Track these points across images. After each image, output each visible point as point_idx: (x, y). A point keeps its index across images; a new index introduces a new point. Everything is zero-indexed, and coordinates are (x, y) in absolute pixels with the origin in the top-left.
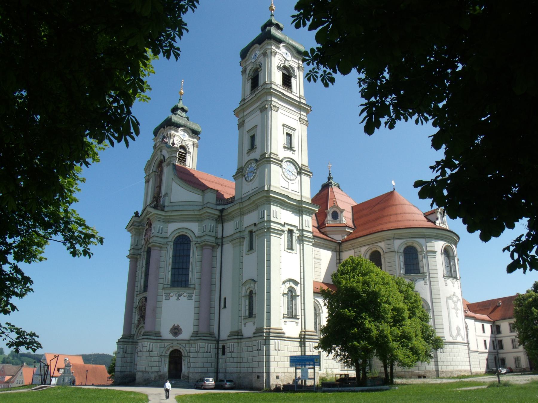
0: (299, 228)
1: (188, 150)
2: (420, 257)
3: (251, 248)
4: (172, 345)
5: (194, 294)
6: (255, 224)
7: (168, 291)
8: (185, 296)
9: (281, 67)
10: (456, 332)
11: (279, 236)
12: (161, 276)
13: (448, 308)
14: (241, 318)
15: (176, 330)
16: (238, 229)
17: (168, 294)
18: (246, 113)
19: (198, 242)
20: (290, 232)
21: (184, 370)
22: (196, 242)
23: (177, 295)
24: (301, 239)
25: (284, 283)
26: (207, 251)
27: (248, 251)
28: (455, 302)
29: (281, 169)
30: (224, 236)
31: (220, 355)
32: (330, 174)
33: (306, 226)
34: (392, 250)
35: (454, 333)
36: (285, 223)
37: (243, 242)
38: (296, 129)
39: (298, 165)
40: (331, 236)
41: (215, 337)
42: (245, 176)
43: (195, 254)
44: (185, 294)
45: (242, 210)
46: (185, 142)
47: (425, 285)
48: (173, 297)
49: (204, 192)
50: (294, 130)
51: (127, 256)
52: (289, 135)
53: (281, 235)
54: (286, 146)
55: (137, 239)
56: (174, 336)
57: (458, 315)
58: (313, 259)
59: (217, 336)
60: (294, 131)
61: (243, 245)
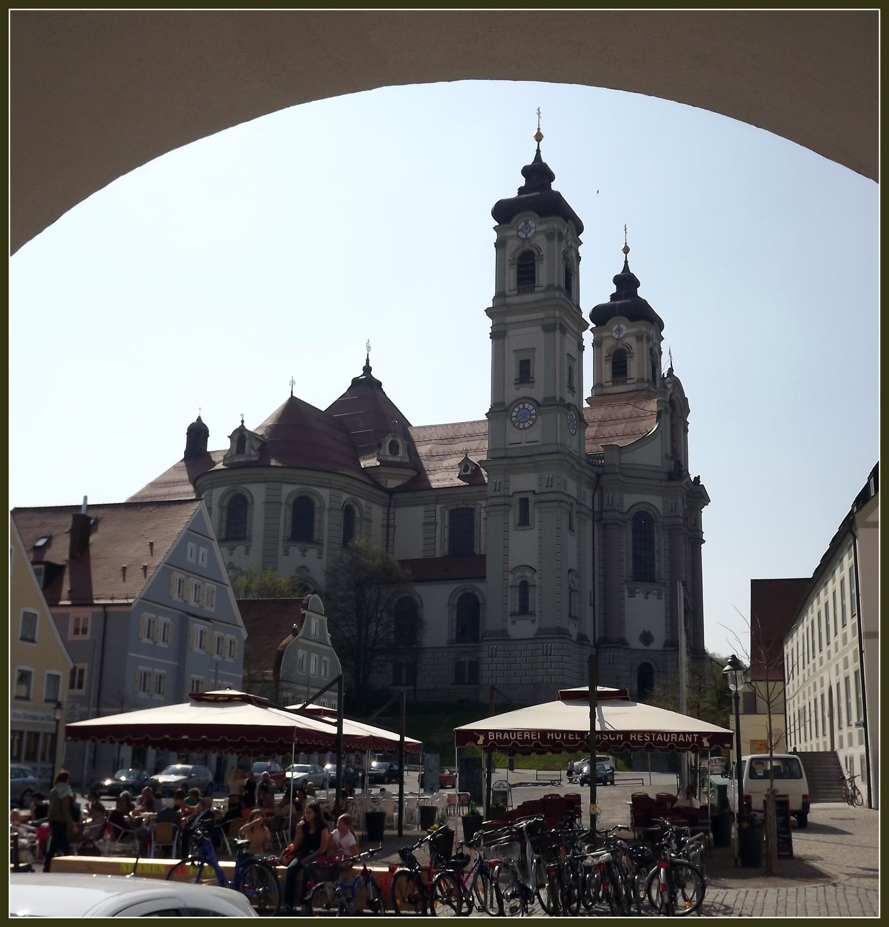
43: (660, 539)
44: (654, 592)
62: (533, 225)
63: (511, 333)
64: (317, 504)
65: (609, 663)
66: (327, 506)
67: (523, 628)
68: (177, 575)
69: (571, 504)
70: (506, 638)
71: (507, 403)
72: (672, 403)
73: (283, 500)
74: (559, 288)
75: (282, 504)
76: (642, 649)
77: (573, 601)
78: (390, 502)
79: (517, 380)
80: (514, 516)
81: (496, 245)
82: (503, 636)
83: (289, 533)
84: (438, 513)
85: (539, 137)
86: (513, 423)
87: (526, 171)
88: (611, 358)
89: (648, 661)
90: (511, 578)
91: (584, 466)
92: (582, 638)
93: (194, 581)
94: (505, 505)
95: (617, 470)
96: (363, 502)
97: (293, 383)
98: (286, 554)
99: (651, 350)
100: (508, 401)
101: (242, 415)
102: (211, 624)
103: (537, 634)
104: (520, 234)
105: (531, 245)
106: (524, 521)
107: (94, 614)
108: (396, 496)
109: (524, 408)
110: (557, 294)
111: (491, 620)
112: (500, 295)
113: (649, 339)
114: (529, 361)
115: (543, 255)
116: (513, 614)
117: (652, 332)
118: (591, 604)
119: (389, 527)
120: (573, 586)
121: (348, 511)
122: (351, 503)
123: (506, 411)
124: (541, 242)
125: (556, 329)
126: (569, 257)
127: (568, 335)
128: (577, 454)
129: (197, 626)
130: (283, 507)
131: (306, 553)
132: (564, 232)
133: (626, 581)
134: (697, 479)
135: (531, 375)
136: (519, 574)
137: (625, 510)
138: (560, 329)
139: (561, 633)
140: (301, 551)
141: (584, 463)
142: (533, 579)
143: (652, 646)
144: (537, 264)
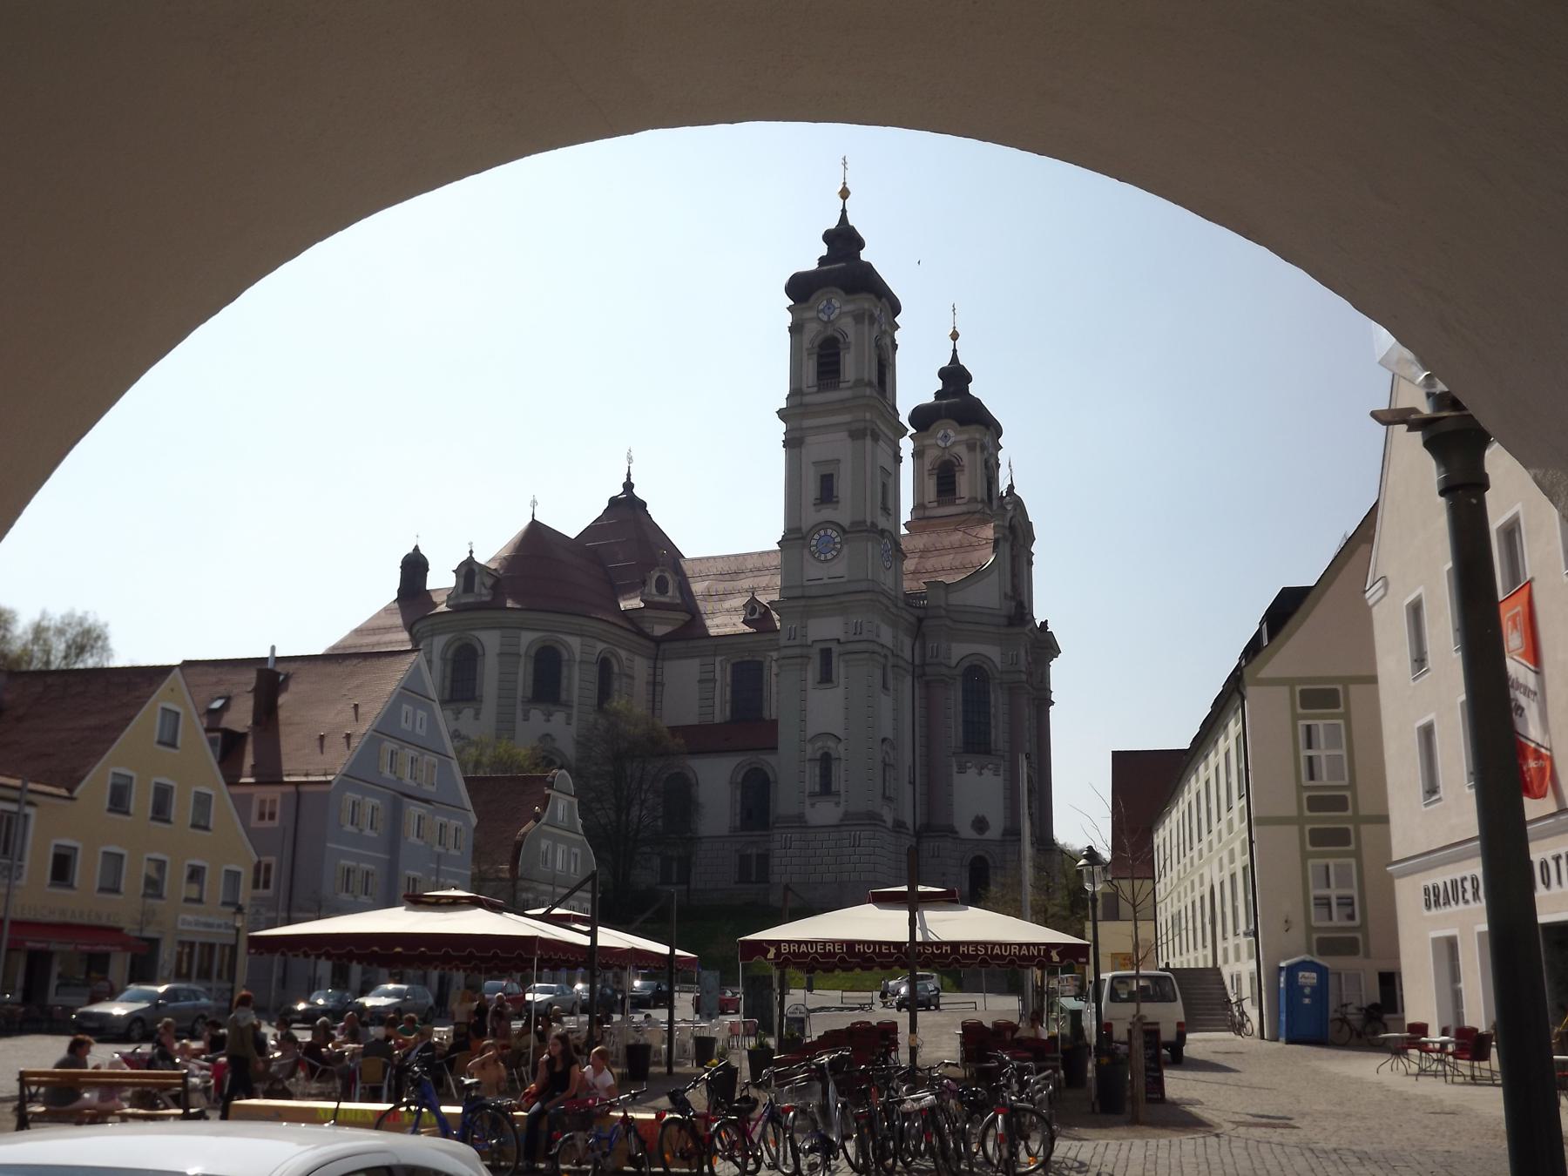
43: (998, 700)
44: (990, 766)
56: (979, 834)
62: (837, 305)
63: (809, 440)
64: (565, 656)
65: (933, 857)
66: (578, 658)
67: (824, 813)
68: (389, 745)
69: (885, 656)
70: (803, 825)
71: (805, 529)
72: (1012, 528)
73: (522, 651)
74: (870, 384)
75: (520, 656)
76: (975, 838)
77: (887, 778)
78: (657, 655)
79: (817, 499)
80: (813, 671)
81: (791, 329)
82: (800, 822)
83: (529, 694)
84: (718, 668)
85: (845, 194)
86: (813, 555)
87: (829, 237)
88: (935, 472)
89: (981, 853)
90: (809, 748)
91: (902, 609)
92: (899, 825)
93: (410, 752)
94: (802, 657)
95: (943, 613)
96: (623, 654)
97: (534, 503)
98: (526, 719)
99: (986, 462)
100: (805, 527)
101: (471, 544)
102: (431, 807)
103: (842, 820)
104: (821, 315)
105: (834, 330)
106: (826, 678)
107: (284, 795)
108: (664, 646)
109: (826, 535)
110: (868, 391)
111: (785, 801)
112: (795, 393)
113: (983, 448)
114: (832, 475)
115: (849, 343)
116: (812, 795)
117: (987, 440)
118: (910, 783)
119: (655, 684)
120: (887, 759)
121: (604, 665)
122: (609, 655)
123: (803, 538)
124: (848, 325)
125: (866, 435)
126: (883, 344)
127: (881, 443)
128: (893, 593)
129: (414, 810)
130: (522, 660)
131: (551, 718)
132: (877, 313)
133: (954, 753)
134: (1044, 624)
135: (835, 494)
136: (819, 744)
137: (953, 662)
138: (872, 436)
139: (873, 818)
140: (545, 715)
141: (901, 604)
142: (838, 750)
143: (988, 835)
144: (841, 354)
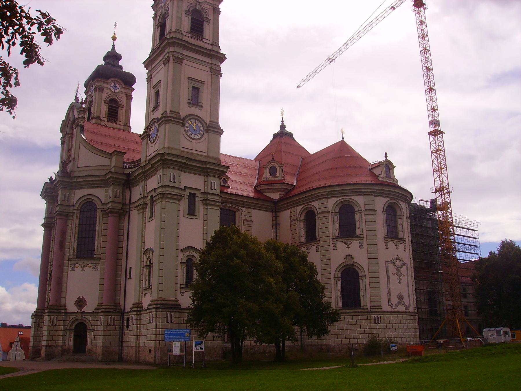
0: (203, 191)
1: (120, 103)
2: (357, 217)
3: (151, 216)
4: (76, 318)
5: (100, 265)
6: (155, 190)
7: (74, 262)
8: (90, 267)
9: (190, 11)
10: (397, 300)
11: (177, 202)
12: (67, 246)
13: (387, 274)
14: (142, 288)
15: (81, 303)
16: (142, 194)
17: (74, 265)
18: (153, 66)
19: (105, 209)
20: (192, 196)
21: (89, 344)
22: (102, 209)
23: (83, 266)
24: (206, 203)
25: (182, 250)
26: (111, 220)
27: (149, 218)
28: (397, 267)
29: (182, 128)
30: (131, 202)
31: (125, 327)
32: (283, 121)
33: (212, 189)
34: (325, 210)
35: (394, 301)
36: (185, 187)
37: (146, 208)
38: (204, 82)
39: (206, 123)
40: (268, 195)
41: (121, 309)
42: (149, 136)
44: (90, 265)
45: (145, 174)
46: (116, 94)
47: (360, 248)
48: (79, 267)
49: (112, 156)
50: (203, 83)
51: (42, 225)
52: (196, 90)
53: (179, 200)
54: (191, 101)
55: (51, 207)
57: (401, 281)
58: (243, 221)
59: (123, 308)
60: (204, 84)
61: (146, 212)
143: (85, 309)
